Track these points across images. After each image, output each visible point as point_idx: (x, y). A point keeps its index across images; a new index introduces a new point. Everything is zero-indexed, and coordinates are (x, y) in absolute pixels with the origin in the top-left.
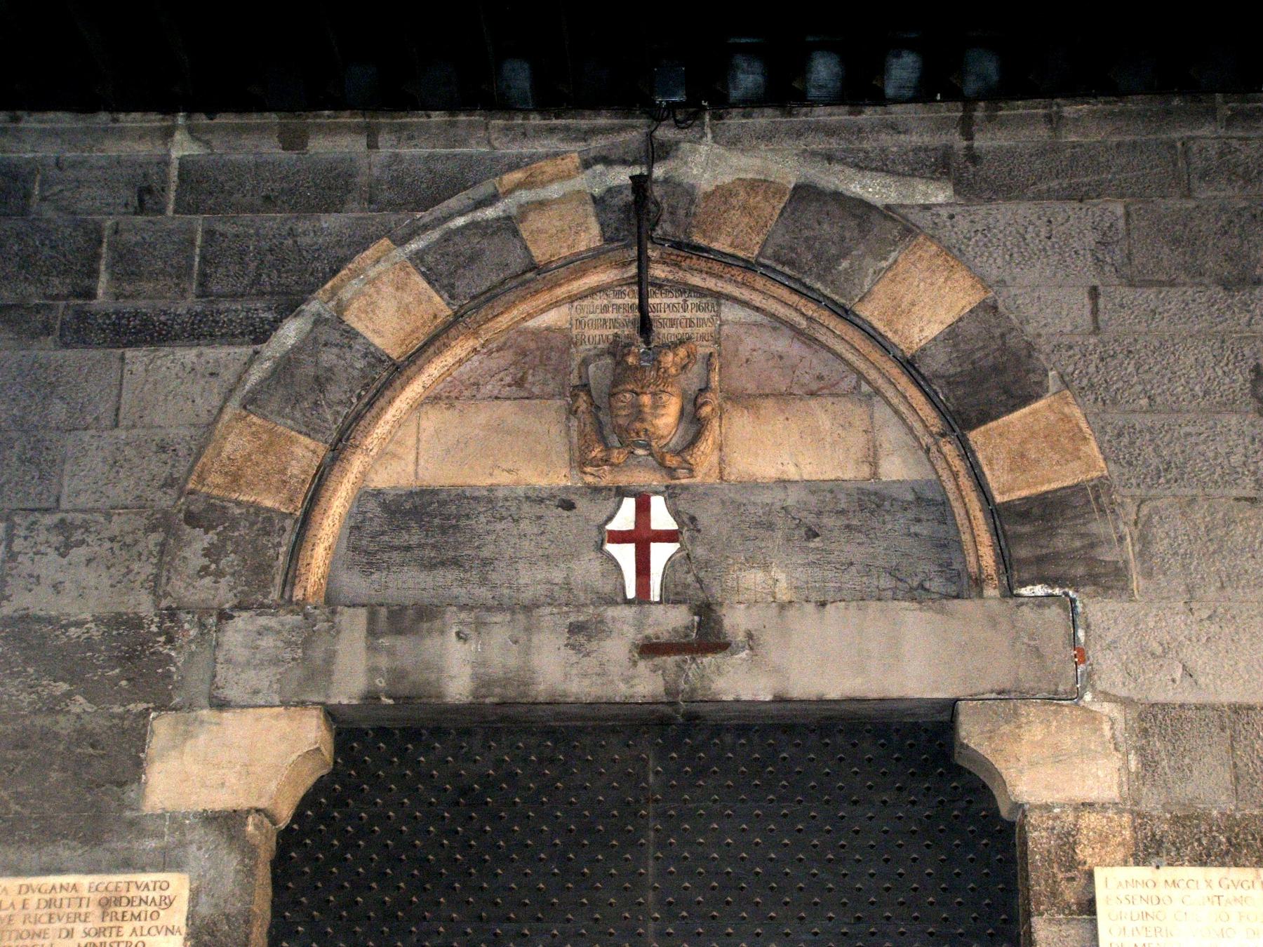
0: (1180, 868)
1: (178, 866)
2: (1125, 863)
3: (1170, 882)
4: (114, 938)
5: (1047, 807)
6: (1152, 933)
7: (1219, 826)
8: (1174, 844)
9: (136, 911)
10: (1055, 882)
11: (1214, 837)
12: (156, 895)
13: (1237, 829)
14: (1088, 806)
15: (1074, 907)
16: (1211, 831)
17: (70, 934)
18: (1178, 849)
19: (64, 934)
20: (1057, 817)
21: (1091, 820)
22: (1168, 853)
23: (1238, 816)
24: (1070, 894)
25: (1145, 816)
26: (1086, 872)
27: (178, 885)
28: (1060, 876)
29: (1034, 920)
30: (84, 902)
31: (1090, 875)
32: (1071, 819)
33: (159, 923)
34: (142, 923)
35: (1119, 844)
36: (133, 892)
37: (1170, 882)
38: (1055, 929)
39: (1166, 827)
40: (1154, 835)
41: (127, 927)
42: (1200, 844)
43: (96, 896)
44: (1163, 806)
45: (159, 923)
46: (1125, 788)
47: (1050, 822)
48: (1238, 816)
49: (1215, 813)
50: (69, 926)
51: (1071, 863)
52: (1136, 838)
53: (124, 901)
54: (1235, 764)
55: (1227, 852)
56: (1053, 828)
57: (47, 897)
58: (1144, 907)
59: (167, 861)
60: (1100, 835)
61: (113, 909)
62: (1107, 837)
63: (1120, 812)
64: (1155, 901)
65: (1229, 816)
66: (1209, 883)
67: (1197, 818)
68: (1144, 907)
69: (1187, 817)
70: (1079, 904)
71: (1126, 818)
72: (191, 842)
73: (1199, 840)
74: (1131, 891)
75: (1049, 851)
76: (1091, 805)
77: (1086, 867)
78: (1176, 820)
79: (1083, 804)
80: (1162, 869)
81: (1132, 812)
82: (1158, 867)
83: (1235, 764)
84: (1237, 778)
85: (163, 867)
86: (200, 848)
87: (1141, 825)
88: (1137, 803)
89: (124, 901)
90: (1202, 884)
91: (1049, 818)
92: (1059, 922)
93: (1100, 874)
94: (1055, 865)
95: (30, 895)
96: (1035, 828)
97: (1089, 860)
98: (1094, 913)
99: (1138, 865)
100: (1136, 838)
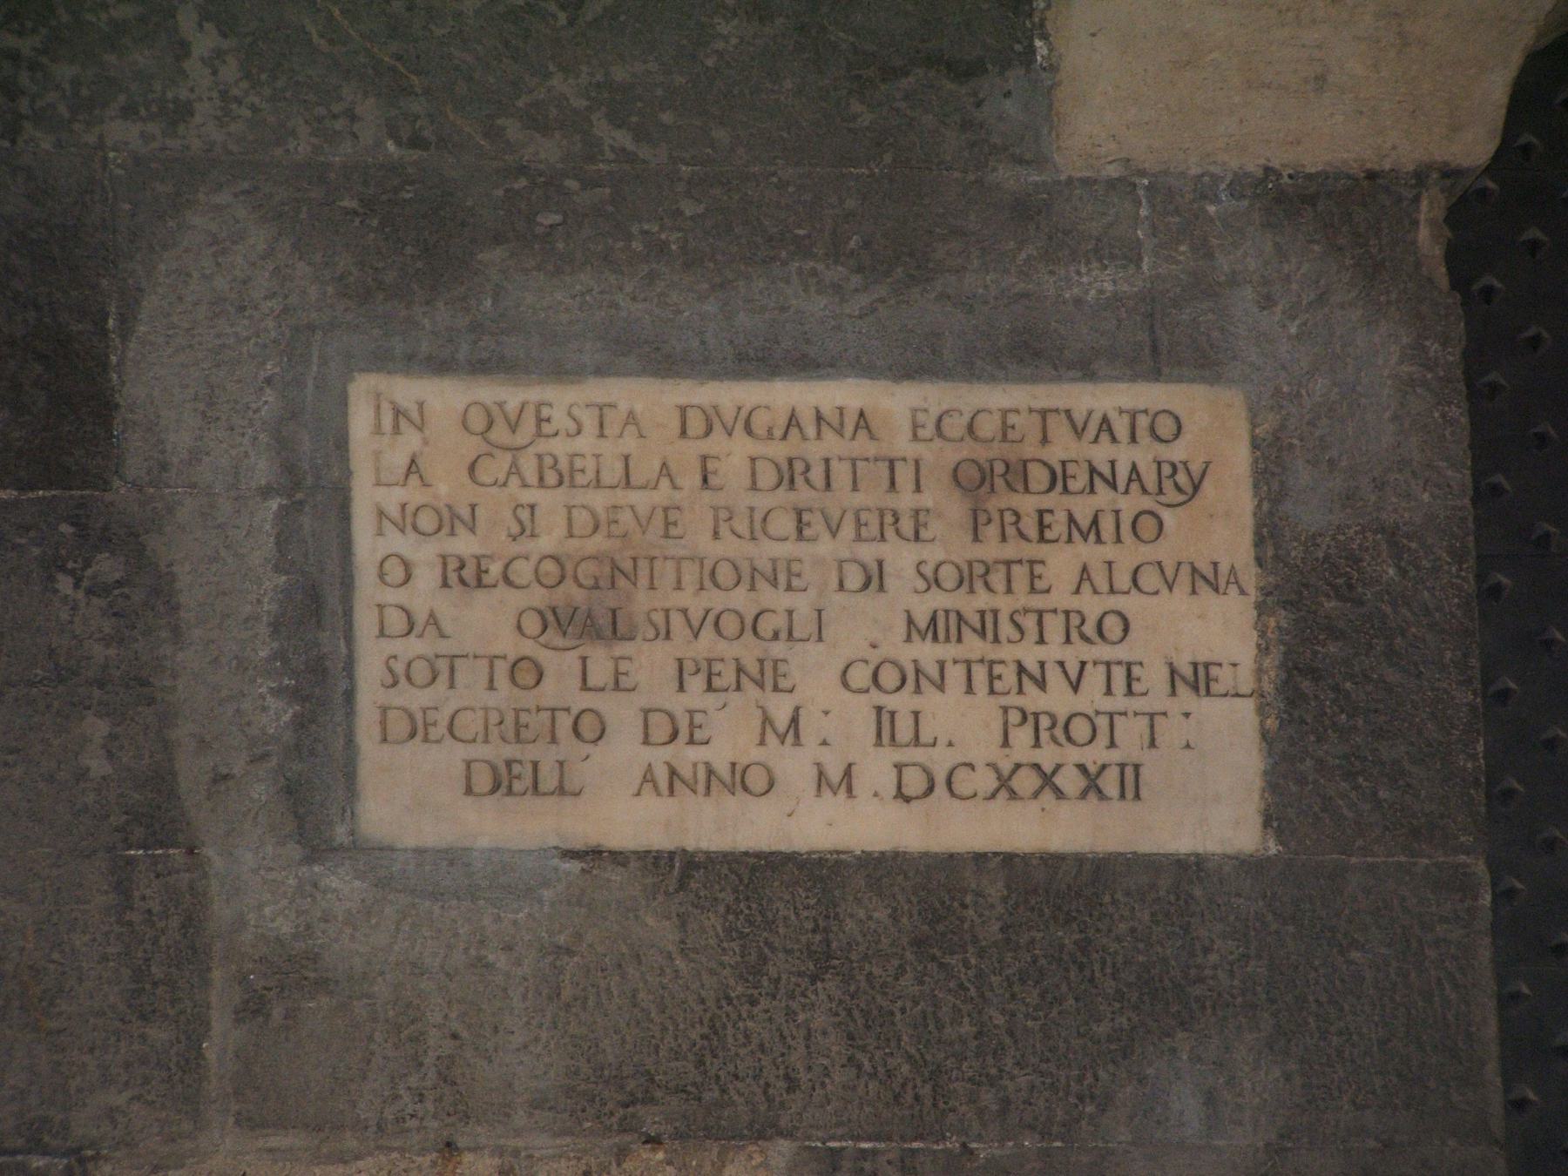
1: (1204, 362)
4: (1022, 599)
9: (1083, 509)
12: (1143, 455)
17: (875, 579)
19: (854, 579)
27: (1212, 424)
30: (904, 475)
33: (1164, 551)
34: (1109, 551)
36: (1063, 447)
41: (1061, 563)
43: (940, 456)
45: (1164, 551)
50: (868, 552)
53: (1038, 476)
57: (779, 451)
59: (1161, 345)
61: (1004, 499)
72: (1233, 281)
85: (1152, 361)
86: (1267, 302)
89: (1038, 476)
95: (717, 443)
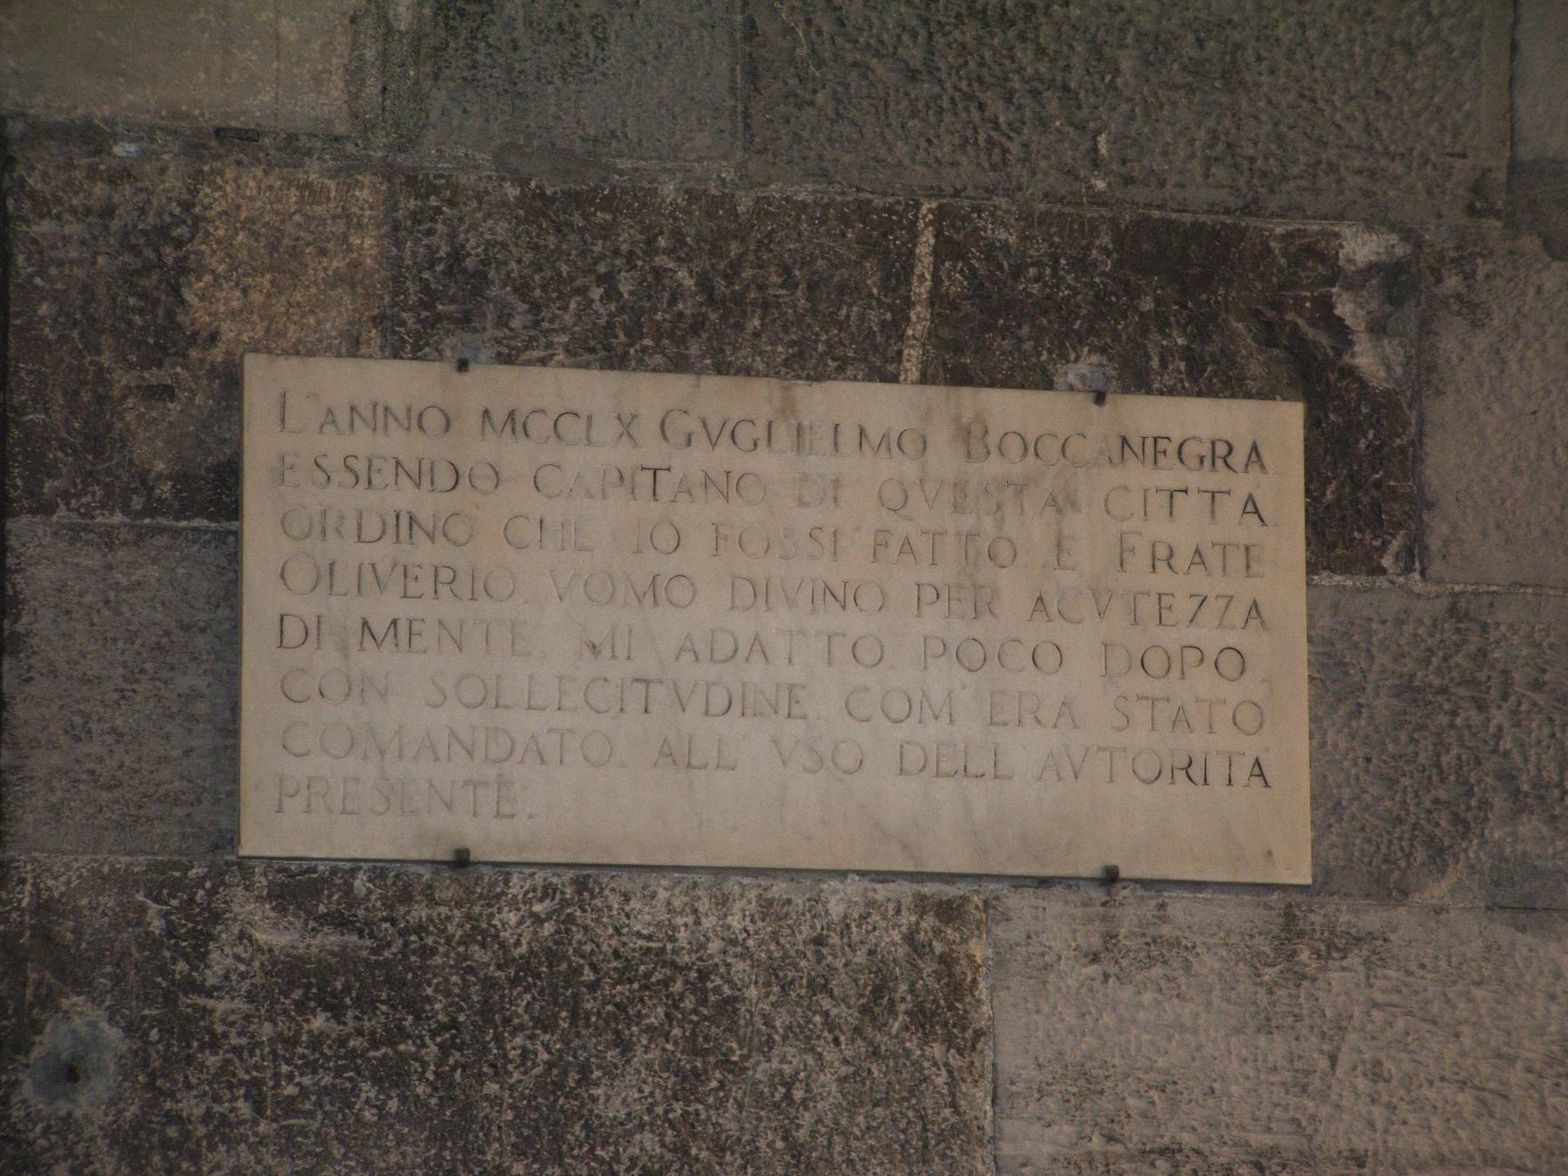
0: (535, 371)
2: (353, 347)
3: (499, 415)
5: (94, 137)
6: (426, 584)
7: (678, 235)
8: (522, 290)
10: (100, 399)
11: (658, 272)
13: (735, 248)
14: (239, 139)
15: (165, 490)
16: (651, 249)
18: (535, 307)
20: (123, 174)
21: (244, 189)
22: (503, 320)
23: (745, 203)
24: (153, 441)
25: (434, 190)
26: (213, 372)
28: (123, 378)
29: (20, 527)
31: (230, 382)
32: (173, 182)
35: (338, 279)
37: (499, 415)
38: (89, 558)
39: (502, 228)
40: (457, 255)
42: (612, 294)
44: (498, 157)
46: (372, 87)
47: (100, 189)
48: (745, 203)
49: (669, 190)
51: (167, 339)
52: (397, 263)
54: (751, 24)
55: (697, 327)
56: (109, 211)
58: (405, 498)
60: (273, 247)
62: (295, 253)
63: (348, 171)
64: (445, 480)
65: (715, 202)
66: (627, 426)
67: (608, 204)
68: (405, 498)
69: (575, 199)
70: (182, 478)
71: (366, 194)
73: (608, 280)
74: (362, 442)
75: (86, 290)
76: (248, 137)
77: (217, 354)
78: (536, 206)
79: (218, 132)
80: (477, 372)
81: (389, 172)
82: (463, 366)
83: (751, 24)
84: (752, 74)
87: (416, 218)
88: (406, 143)
90: (606, 430)
91: (93, 173)
92: (108, 539)
93: (263, 380)
94: (106, 340)
96: (42, 207)
97: (228, 330)
98: (234, 511)
99: (396, 355)
100: (397, 263)
